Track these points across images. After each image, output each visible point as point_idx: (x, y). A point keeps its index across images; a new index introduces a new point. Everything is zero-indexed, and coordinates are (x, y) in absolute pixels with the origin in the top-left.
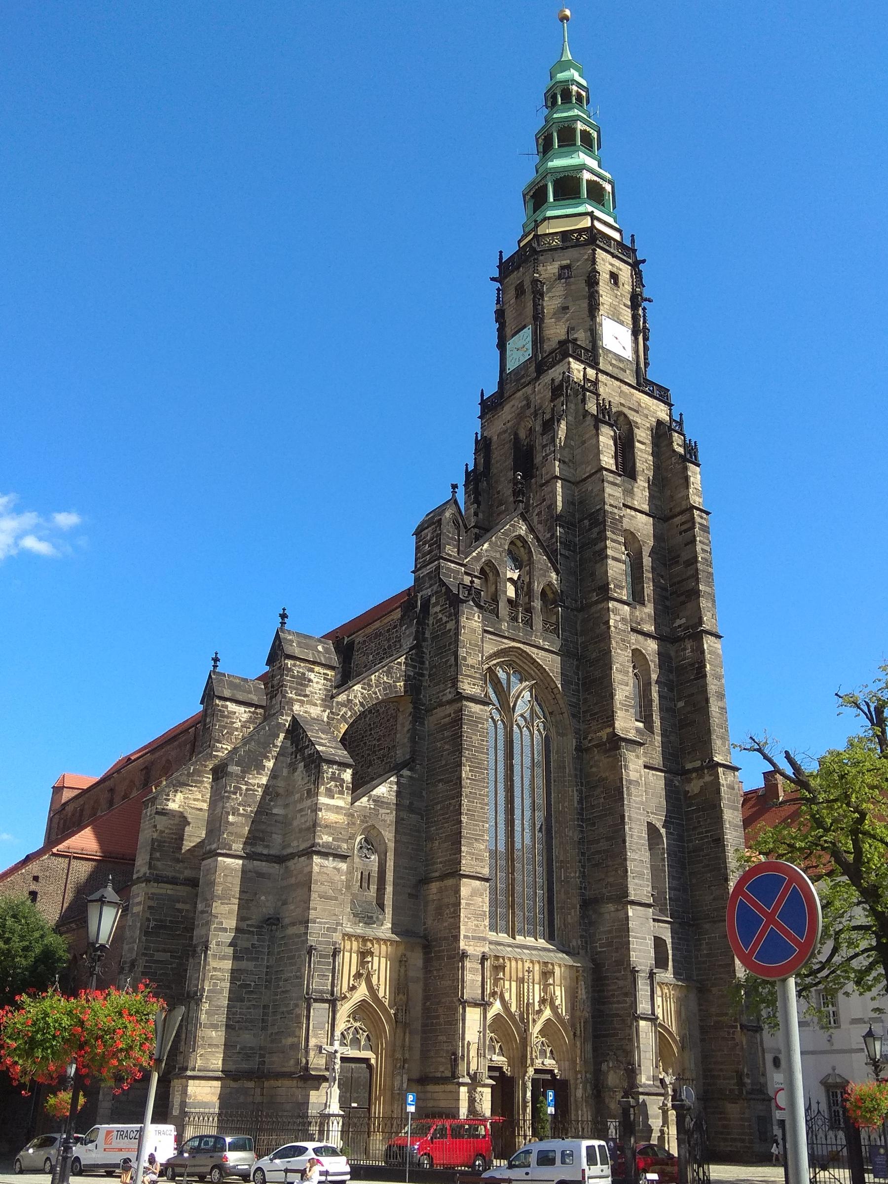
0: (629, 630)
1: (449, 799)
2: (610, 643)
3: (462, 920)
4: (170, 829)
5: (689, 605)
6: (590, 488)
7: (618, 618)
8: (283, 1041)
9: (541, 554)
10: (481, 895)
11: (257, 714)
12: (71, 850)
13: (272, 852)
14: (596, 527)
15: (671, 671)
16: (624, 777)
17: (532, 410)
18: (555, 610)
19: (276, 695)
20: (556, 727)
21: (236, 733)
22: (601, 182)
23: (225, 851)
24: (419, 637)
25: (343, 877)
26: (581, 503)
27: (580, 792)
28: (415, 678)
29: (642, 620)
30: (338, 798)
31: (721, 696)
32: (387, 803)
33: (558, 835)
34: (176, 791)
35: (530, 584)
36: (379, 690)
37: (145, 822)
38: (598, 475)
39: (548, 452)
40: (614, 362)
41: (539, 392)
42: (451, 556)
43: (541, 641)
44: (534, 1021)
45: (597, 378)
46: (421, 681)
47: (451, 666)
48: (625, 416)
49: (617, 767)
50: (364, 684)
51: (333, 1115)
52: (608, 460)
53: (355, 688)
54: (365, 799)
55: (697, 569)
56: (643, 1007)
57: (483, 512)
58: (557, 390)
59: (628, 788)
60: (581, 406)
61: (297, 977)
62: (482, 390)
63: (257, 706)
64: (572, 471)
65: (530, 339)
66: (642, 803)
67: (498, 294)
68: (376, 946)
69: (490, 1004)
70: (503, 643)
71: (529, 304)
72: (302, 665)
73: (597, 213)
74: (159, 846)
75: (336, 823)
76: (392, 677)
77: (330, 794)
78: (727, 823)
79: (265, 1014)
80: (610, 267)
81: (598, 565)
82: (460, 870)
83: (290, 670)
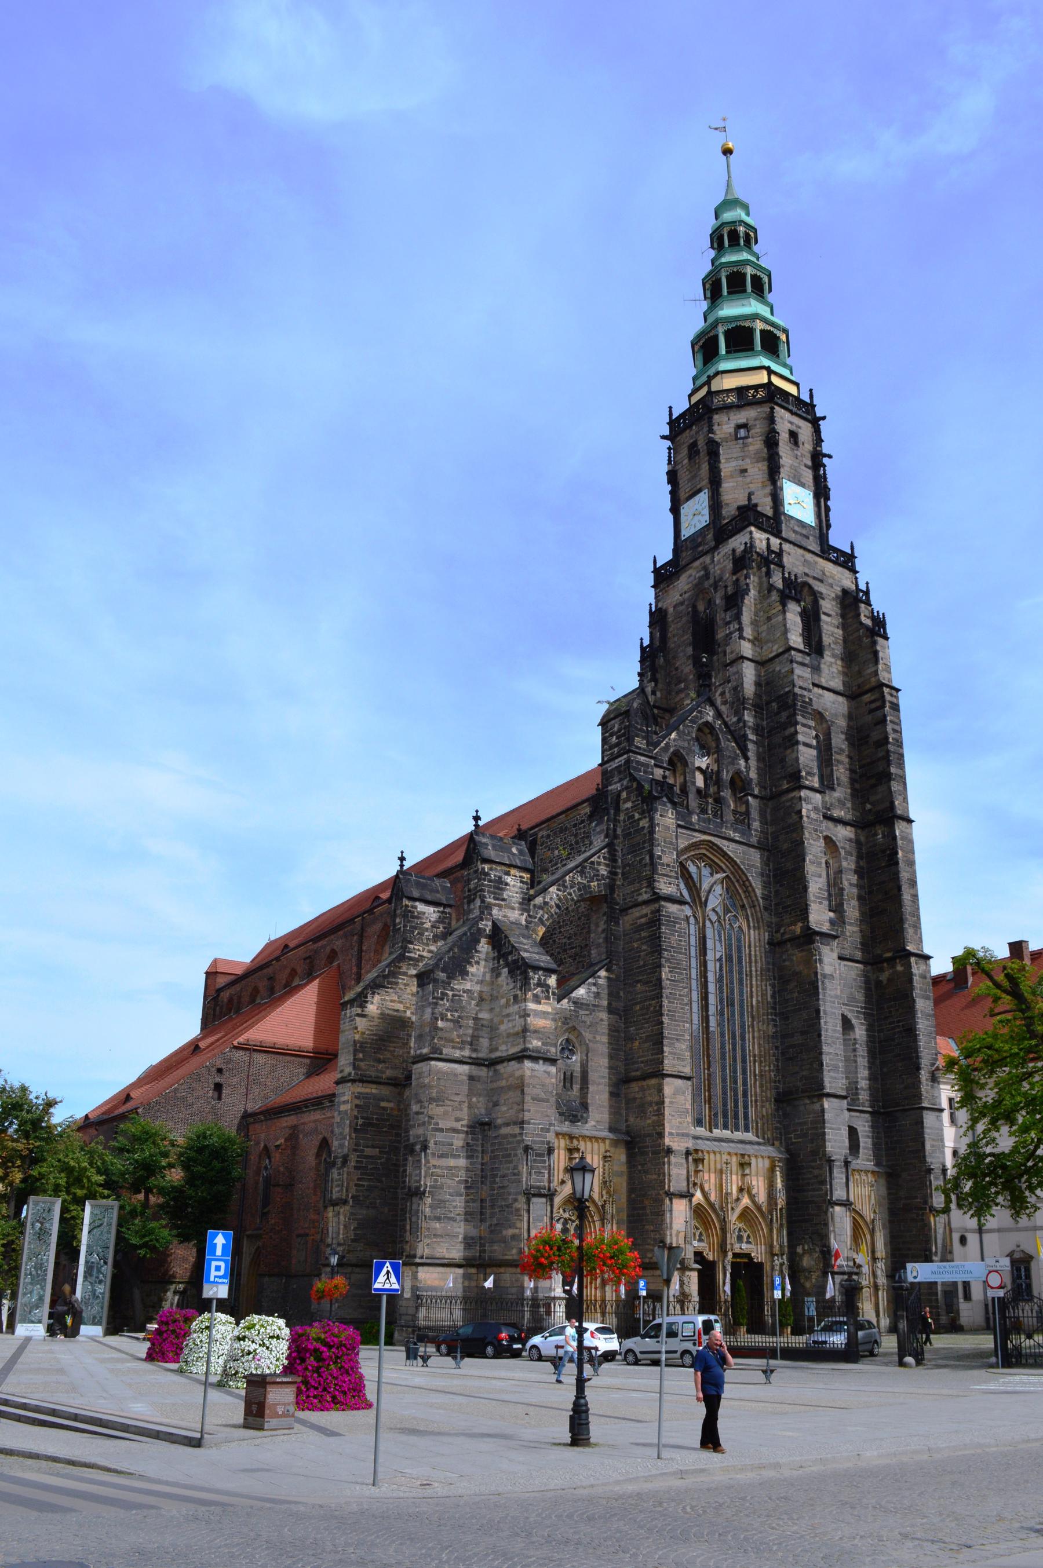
0: (822, 818)
1: (649, 1000)
2: (803, 834)
3: (666, 1117)
4: (371, 1030)
5: (881, 789)
6: (777, 669)
7: (810, 807)
8: (504, 1232)
9: (729, 741)
10: (684, 1093)
11: (446, 913)
12: (250, 1043)
13: (481, 1055)
14: (785, 710)
15: (862, 859)
16: (819, 971)
17: (711, 581)
18: (745, 798)
19: (474, 899)
20: (748, 920)
21: (426, 933)
22: (775, 331)
23: (436, 1056)
24: (612, 836)
25: (553, 1080)
26: (768, 684)
27: (773, 986)
29: (831, 805)
30: (544, 1003)
31: (913, 883)
32: (588, 1005)
34: (373, 993)
35: (718, 772)
36: (574, 891)
37: (344, 1023)
38: (786, 655)
39: (732, 629)
40: (796, 528)
41: (719, 561)
42: (639, 748)
43: (731, 832)
44: (733, 1209)
45: (781, 549)
46: (614, 880)
47: (645, 865)
48: (810, 587)
49: (811, 962)
50: (559, 885)
51: (560, 1298)
52: (796, 639)
53: (551, 889)
54: (566, 1001)
55: (888, 751)
56: (839, 1193)
57: (661, 690)
58: (741, 562)
59: (823, 982)
60: (764, 579)
61: (514, 1174)
62: (655, 557)
63: (445, 906)
64: (758, 649)
65: (706, 504)
66: (836, 997)
67: (670, 453)
68: (582, 1143)
69: (692, 1195)
71: (704, 466)
72: (499, 868)
73: (775, 367)
74: (361, 1047)
75: (544, 1028)
76: (586, 877)
77: (537, 1000)
78: (919, 1012)
79: (482, 1207)
80: (789, 425)
81: (789, 751)
82: (663, 1070)
83: (487, 874)
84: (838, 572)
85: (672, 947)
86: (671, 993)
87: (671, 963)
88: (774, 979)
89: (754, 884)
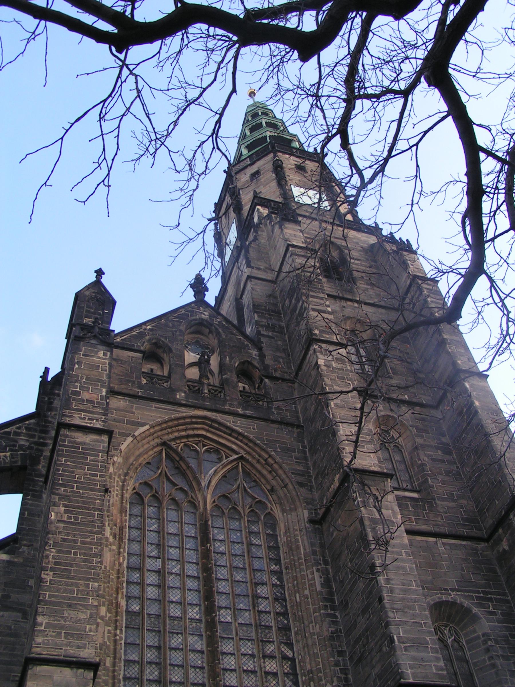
27: (326, 572)
28: (30, 448)
33: (299, 637)
70: (179, 411)
84: (362, 236)
85: (76, 482)
86: (64, 540)
87: (70, 501)
88: (326, 563)
89: (278, 459)
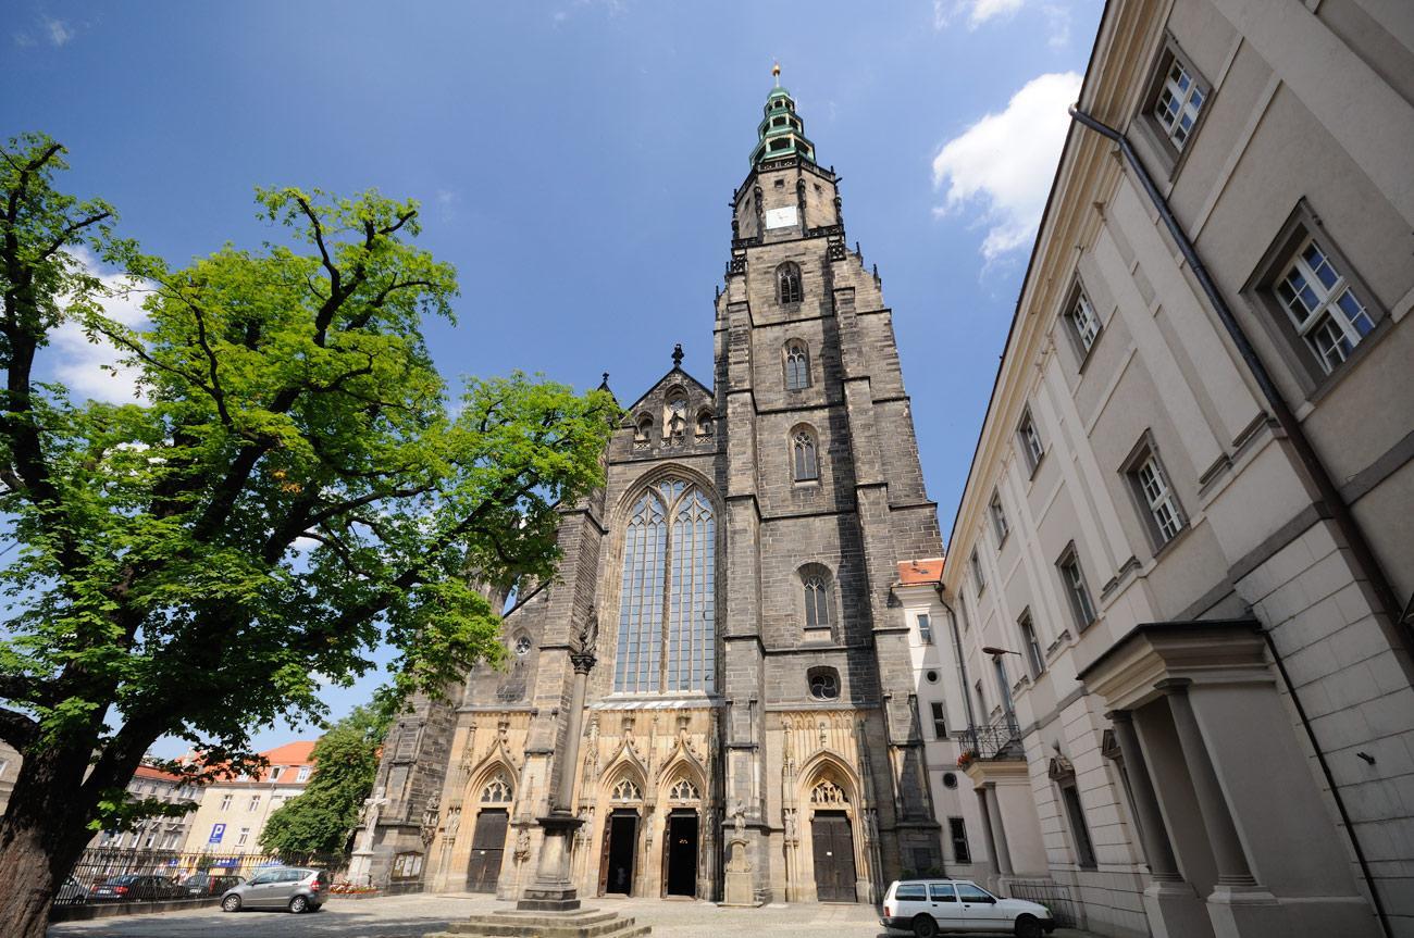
10: (559, 661)
48: (792, 262)
